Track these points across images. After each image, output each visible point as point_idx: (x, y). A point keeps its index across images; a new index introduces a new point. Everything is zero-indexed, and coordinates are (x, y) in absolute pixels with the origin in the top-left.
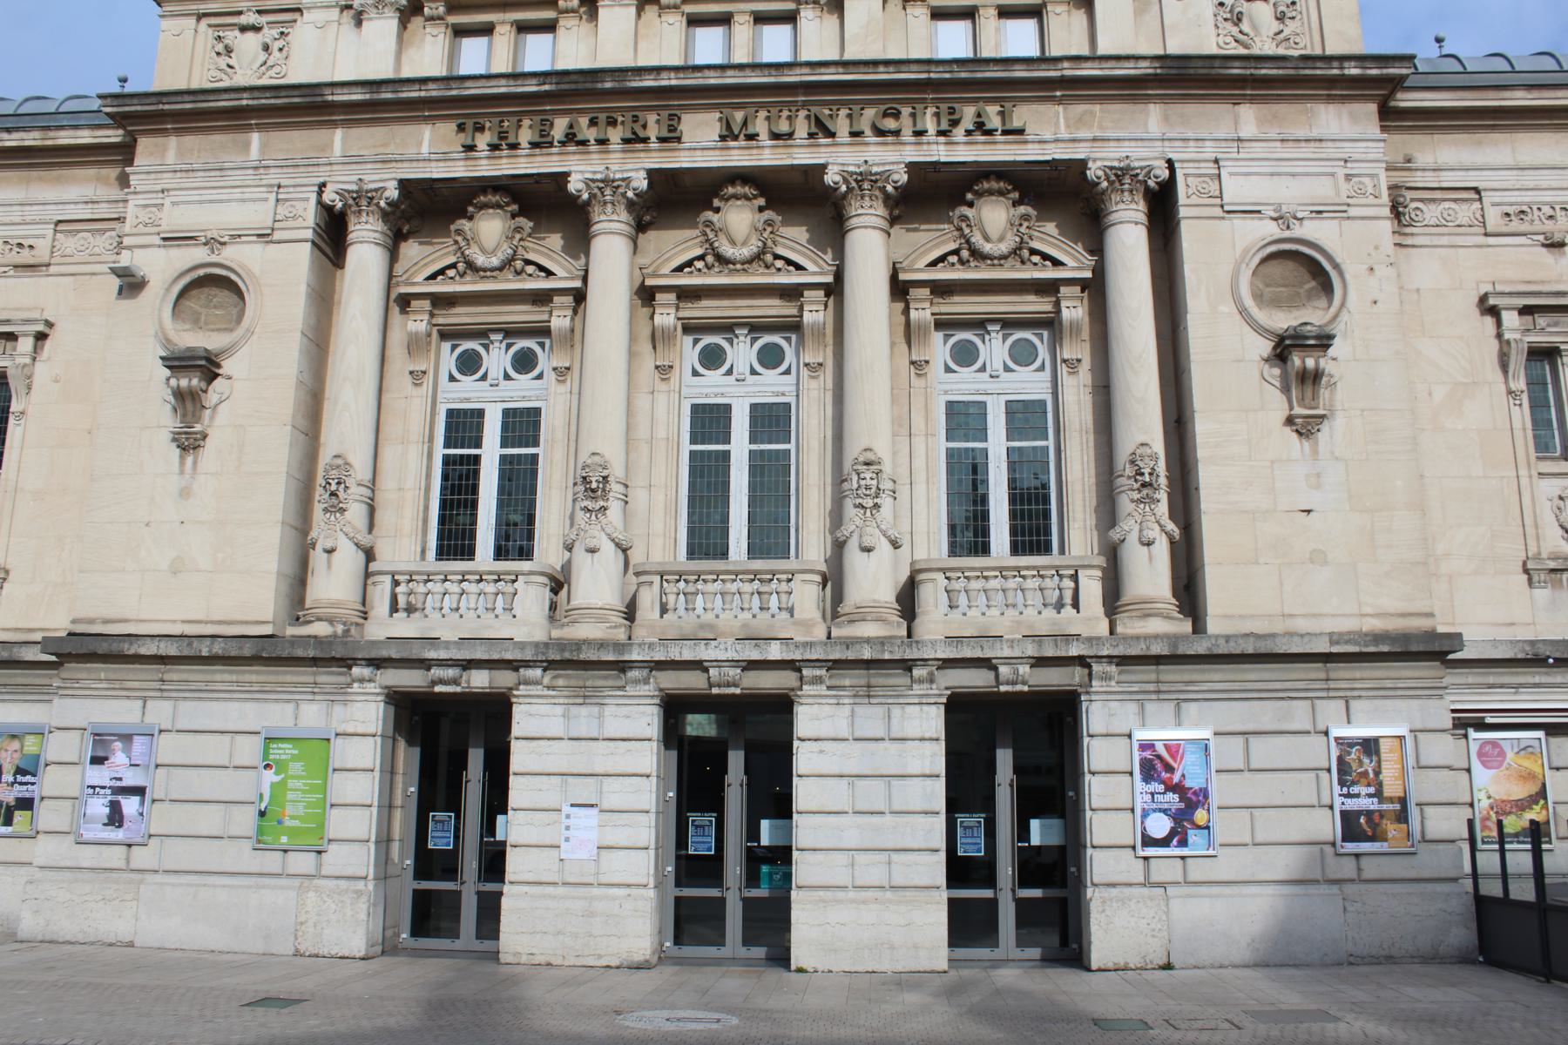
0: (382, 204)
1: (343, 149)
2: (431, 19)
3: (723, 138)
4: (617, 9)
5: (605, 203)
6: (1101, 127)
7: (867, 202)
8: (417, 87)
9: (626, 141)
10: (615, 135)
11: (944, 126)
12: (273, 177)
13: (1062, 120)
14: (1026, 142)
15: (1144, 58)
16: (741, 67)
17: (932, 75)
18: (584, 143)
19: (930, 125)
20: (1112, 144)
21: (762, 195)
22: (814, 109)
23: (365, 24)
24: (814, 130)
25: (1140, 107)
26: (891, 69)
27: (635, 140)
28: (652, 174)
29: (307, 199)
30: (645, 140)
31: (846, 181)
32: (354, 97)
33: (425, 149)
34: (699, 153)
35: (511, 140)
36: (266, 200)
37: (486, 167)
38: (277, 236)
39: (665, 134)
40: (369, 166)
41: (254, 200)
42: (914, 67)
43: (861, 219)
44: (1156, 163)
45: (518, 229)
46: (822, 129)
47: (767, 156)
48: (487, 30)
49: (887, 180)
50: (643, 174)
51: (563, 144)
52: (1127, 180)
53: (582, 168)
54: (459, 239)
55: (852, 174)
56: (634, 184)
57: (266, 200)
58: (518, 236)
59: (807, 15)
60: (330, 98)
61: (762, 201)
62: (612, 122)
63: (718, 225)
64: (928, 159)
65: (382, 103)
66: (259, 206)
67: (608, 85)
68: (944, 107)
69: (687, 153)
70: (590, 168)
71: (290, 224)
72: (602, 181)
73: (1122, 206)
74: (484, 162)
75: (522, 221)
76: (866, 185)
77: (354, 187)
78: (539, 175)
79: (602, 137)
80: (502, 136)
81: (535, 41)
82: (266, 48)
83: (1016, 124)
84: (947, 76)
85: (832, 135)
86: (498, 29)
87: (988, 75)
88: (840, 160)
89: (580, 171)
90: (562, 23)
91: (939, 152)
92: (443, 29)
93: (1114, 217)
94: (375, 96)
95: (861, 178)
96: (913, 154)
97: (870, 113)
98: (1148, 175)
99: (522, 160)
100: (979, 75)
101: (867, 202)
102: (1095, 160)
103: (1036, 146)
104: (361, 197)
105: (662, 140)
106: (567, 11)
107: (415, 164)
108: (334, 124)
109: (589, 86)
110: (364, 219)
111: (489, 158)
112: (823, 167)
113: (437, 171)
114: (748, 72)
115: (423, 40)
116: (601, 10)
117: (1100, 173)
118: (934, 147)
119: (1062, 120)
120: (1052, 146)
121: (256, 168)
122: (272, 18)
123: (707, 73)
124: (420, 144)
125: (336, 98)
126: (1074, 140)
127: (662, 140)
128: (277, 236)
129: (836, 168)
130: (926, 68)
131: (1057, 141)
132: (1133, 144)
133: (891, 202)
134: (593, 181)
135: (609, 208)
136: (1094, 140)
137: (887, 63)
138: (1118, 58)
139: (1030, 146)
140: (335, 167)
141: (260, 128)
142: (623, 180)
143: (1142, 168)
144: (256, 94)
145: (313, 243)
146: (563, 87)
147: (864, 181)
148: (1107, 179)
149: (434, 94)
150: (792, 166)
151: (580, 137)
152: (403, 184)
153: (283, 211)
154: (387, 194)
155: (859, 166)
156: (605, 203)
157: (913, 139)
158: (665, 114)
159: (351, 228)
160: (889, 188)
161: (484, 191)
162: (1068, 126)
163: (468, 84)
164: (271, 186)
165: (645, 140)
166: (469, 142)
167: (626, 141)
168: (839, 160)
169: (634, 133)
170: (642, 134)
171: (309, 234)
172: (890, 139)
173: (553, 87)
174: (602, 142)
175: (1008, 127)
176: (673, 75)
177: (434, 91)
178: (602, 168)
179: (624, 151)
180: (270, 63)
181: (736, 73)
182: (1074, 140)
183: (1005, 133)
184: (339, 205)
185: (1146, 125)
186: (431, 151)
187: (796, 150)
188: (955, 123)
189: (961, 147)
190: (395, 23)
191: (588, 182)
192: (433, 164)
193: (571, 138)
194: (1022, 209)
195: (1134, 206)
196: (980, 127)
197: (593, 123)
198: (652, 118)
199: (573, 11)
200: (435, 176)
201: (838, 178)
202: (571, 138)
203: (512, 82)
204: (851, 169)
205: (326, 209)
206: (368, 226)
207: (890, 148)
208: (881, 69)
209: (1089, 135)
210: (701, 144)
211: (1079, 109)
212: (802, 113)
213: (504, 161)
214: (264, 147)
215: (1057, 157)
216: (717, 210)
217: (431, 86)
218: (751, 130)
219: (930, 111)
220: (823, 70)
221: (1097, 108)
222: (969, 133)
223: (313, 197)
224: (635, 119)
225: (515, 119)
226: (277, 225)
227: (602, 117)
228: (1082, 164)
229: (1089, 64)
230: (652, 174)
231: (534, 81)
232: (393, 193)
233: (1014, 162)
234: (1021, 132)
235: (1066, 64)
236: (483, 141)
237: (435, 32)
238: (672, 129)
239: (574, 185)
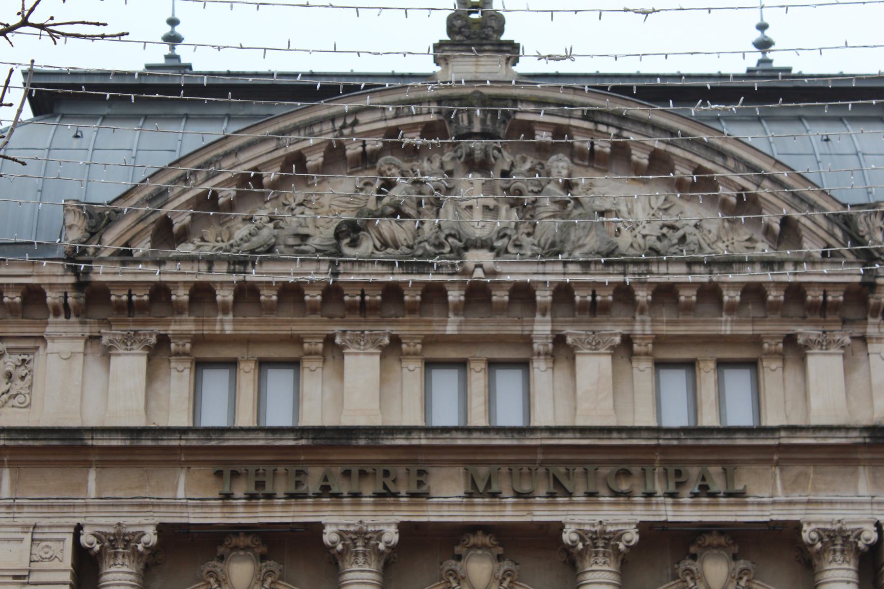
0: (140, 547)
1: (99, 489)
2: (177, 354)
3: (469, 495)
4: (362, 357)
5: (357, 554)
6: (815, 489)
7: (601, 559)
8: (178, 436)
9: (378, 495)
10: (368, 489)
11: (672, 488)
12: (27, 517)
13: (779, 482)
14: (746, 504)
15: (854, 429)
16: (485, 430)
17: (661, 442)
18: (337, 496)
19: (659, 488)
20: (825, 506)
21: (500, 545)
22: (553, 469)
23: (113, 360)
24: (552, 490)
25: (850, 469)
26: (624, 435)
27: (385, 495)
28: (404, 528)
29: (63, 540)
30: (396, 495)
31: (582, 539)
32: (114, 443)
33: (181, 494)
34: (445, 508)
35: (268, 490)
36: (21, 540)
37: (241, 516)
38: (34, 578)
39: (414, 489)
40: (126, 509)
41: (9, 540)
42: (645, 434)
43: (596, 574)
44: (866, 527)
45: (270, 573)
46: (559, 490)
47: (509, 513)
48: (232, 364)
49: (619, 538)
50: (393, 529)
51: (318, 496)
52: (839, 541)
53: (335, 520)
54: (212, 580)
55: (587, 532)
56: (386, 538)
57: (21, 540)
58: (269, 580)
59: (540, 370)
60: (90, 443)
61: (500, 551)
62: (363, 474)
63: (461, 574)
64: (657, 519)
65: (141, 449)
66: (13, 546)
67: (362, 442)
68: (671, 470)
69: (434, 508)
70: (343, 520)
71: (46, 565)
72: (355, 533)
73: (834, 565)
74: (241, 510)
75: (272, 564)
76: (601, 543)
77: (111, 530)
78: (293, 523)
79: (355, 490)
80: (260, 485)
81: (279, 382)
82: (9, 376)
83: (739, 487)
84: (675, 442)
85: (570, 495)
86: (242, 366)
87: (712, 442)
88: (577, 519)
89: (334, 522)
90: (306, 364)
91: (666, 512)
92: (188, 365)
93: (828, 576)
94: (136, 443)
95: (595, 537)
96: (642, 514)
97: (604, 471)
98: (858, 537)
99: (278, 509)
100: (704, 442)
101: (601, 559)
102: (809, 523)
103: (756, 508)
104: (119, 541)
105: (412, 495)
106: (310, 354)
107: (171, 509)
108: (88, 464)
109: (343, 442)
110: (120, 560)
111: (245, 506)
112: (560, 527)
113: (195, 517)
114: (492, 435)
115: (170, 374)
116: (346, 357)
117: (814, 535)
118: (662, 508)
119: (779, 482)
120: (770, 508)
121: (9, 506)
122: (11, 345)
123: (455, 434)
124: (176, 488)
125: (95, 443)
126: (790, 503)
127: (412, 495)
128: (34, 578)
129: (573, 528)
130: (656, 435)
131: (774, 503)
132: (844, 507)
133: (620, 558)
134: (346, 532)
135: (361, 559)
136: (809, 502)
137: (620, 430)
138: (830, 428)
139: (750, 508)
140: (91, 509)
141: (11, 464)
142: (375, 532)
143: (853, 531)
144: (14, 436)
145: (71, 585)
146: (319, 442)
147: (601, 540)
148: (821, 539)
149: (194, 443)
150: (532, 523)
151: (335, 490)
152: (162, 529)
153: (38, 551)
154: (145, 539)
155: (593, 525)
156: (357, 554)
157: (642, 499)
158: (414, 469)
159: (106, 569)
160: (622, 546)
161: (237, 534)
162: (784, 488)
163: (227, 436)
164: (28, 526)
165: (396, 495)
166: (227, 490)
167: (378, 495)
168: (576, 518)
169: (385, 487)
170: (393, 489)
171: (67, 577)
172: (622, 499)
173: (310, 442)
174: (356, 495)
175: (730, 490)
176: (422, 435)
177: (193, 441)
178: (355, 520)
179: (375, 504)
180: (13, 392)
181: (483, 435)
182: (790, 503)
183: (728, 495)
184: (97, 547)
185: (856, 487)
186: (188, 499)
187: (536, 508)
188: (679, 485)
189: (687, 508)
190: (143, 360)
191: (341, 534)
192: (190, 510)
193: (325, 490)
194: (742, 564)
195: (846, 566)
196: (705, 490)
197: (347, 474)
198: (401, 471)
199: (316, 353)
200: (192, 521)
201: (575, 537)
202: (325, 490)
203: (270, 436)
204: (587, 528)
205: (80, 552)
206: (125, 569)
207: (622, 507)
208: (615, 435)
209: (805, 499)
210: (448, 503)
211: (796, 470)
212: (541, 470)
213: (260, 509)
214: (14, 483)
215: (775, 518)
216: (459, 558)
217: (191, 436)
218: (495, 488)
219: (659, 470)
220: (561, 435)
221: (811, 470)
222: (695, 495)
223: (69, 539)
224: (386, 473)
225: (270, 469)
226: (35, 566)
227: (355, 470)
228: (797, 526)
229: (803, 434)
230: (404, 528)
231: (292, 436)
232: (151, 537)
233: (735, 523)
234: (741, 494)
235: (783, 434)
236: (240, 490)
237: (180, 367)
238: (420, 483)
239: (329, 536)
